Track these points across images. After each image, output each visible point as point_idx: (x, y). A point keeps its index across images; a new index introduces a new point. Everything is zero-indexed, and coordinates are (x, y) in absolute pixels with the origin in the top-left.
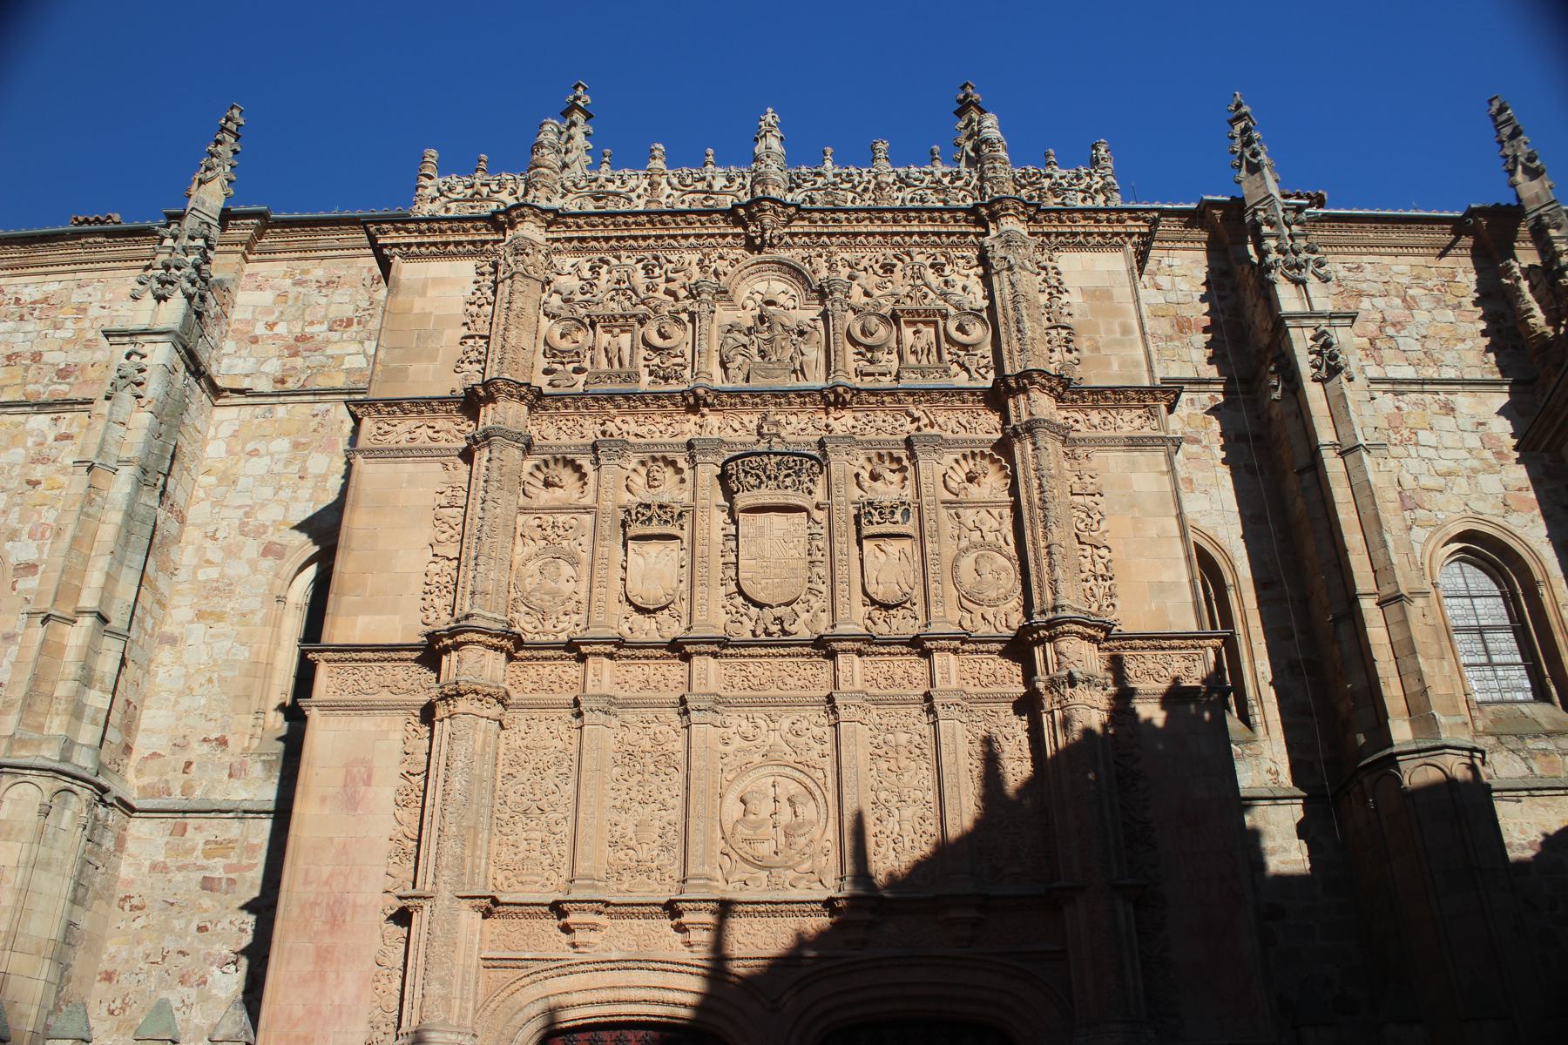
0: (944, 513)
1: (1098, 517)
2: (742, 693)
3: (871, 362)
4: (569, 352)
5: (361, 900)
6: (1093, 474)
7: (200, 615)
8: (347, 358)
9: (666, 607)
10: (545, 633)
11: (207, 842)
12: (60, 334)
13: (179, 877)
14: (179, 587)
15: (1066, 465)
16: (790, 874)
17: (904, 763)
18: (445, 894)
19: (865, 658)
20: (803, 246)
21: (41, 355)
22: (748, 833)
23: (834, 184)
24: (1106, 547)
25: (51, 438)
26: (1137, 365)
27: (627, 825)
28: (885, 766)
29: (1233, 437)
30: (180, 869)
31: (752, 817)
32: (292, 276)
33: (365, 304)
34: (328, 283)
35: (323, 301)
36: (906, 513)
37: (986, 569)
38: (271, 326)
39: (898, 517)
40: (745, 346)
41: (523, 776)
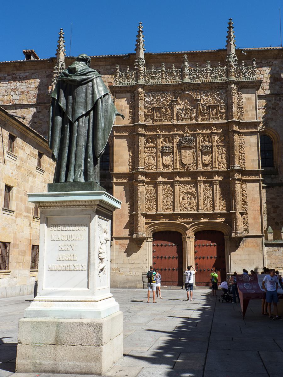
0: (216, 148)
3: (205, 116)
5: (125, 213)
6: (243, 139)
10: (150, 170)
15: (239, 137)
16: (191, 209)
17: (208, 191)
18: (139, 213)
20: (193, 90)
23: (198, 73)
27: (165, 201)
28: (205, 192)
37: (223, 157)
39: (209, 149)
40: (182, 113)
41: (148, 194)
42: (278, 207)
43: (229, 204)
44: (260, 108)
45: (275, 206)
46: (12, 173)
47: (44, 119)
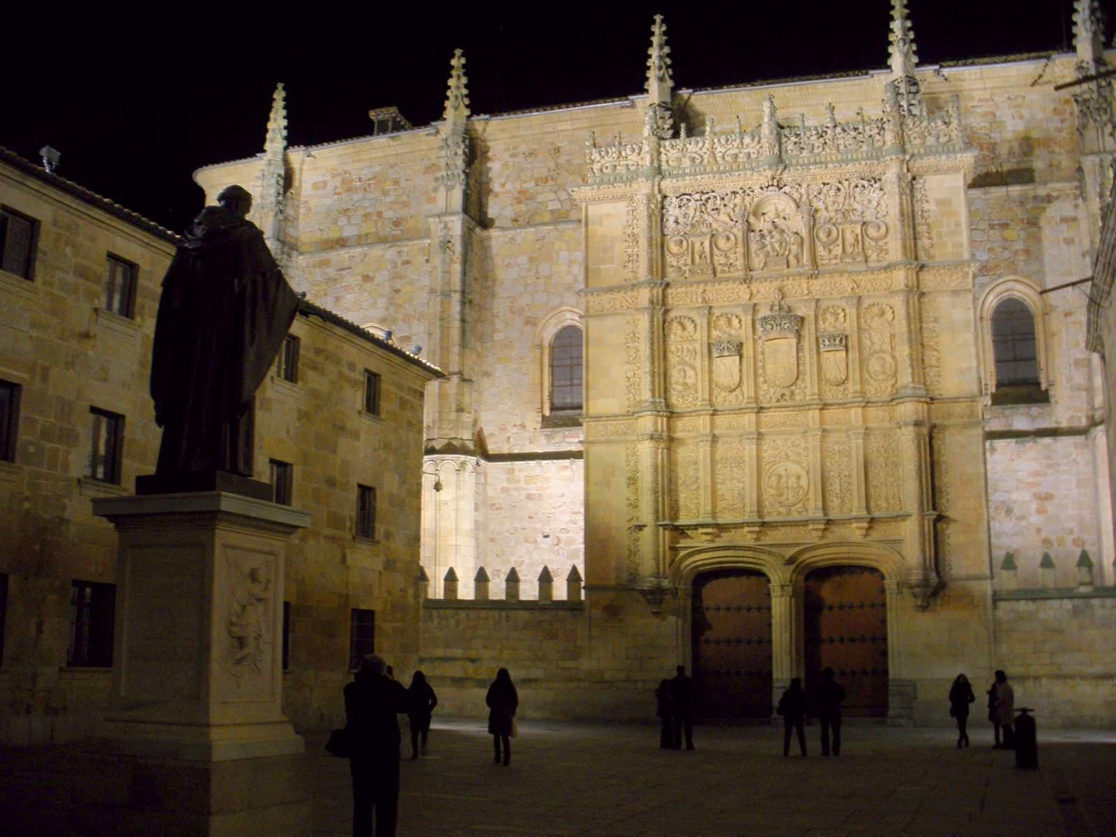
1: (935, 335)
2: (771, 429)
4: (677, 255)
7: (499, 359)
8: (550, 203)
9: (735, 390)
11: (526, 477)
12: (389, 199)
13: (515, 494)
14: (485, 345)
19: (825, 411)
21: (381, 213)
22: (773, 492)
24: (936, 350)
25: (400, 264)
26: (961, 245)
29: (1058, 220)
30: (515, 489)
31: (775, 485)
32: (508, 149)
33: (552, 165)
34: (530, 154)
35: (529, 166)
36: (841, 340)
38: (503, 185)
39: (837, 342)
42: (1048, 497)
43: (896, 492)
44: (996, 222)
45: (1043, 495)
46: (288, 432)
47: (418, 280)
